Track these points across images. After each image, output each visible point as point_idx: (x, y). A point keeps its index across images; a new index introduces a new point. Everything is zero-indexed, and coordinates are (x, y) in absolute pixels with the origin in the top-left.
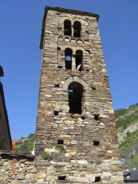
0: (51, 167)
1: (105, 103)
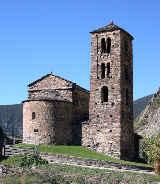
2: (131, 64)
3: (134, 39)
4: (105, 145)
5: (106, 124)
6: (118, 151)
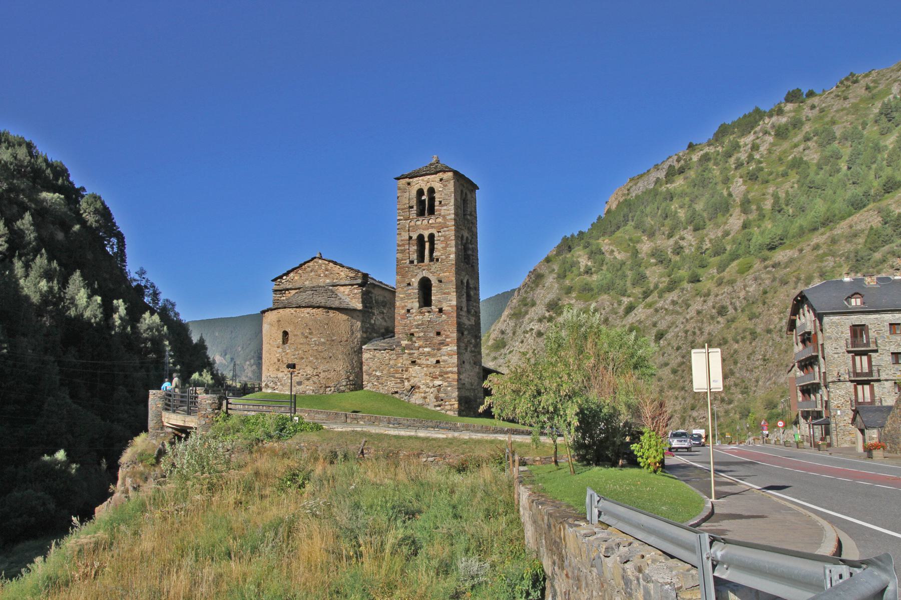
0: (406, 355)
2: (474, 235)
3: (478, 189)
4: (428, 390)
5: (427, 350)
6: (454, 400)
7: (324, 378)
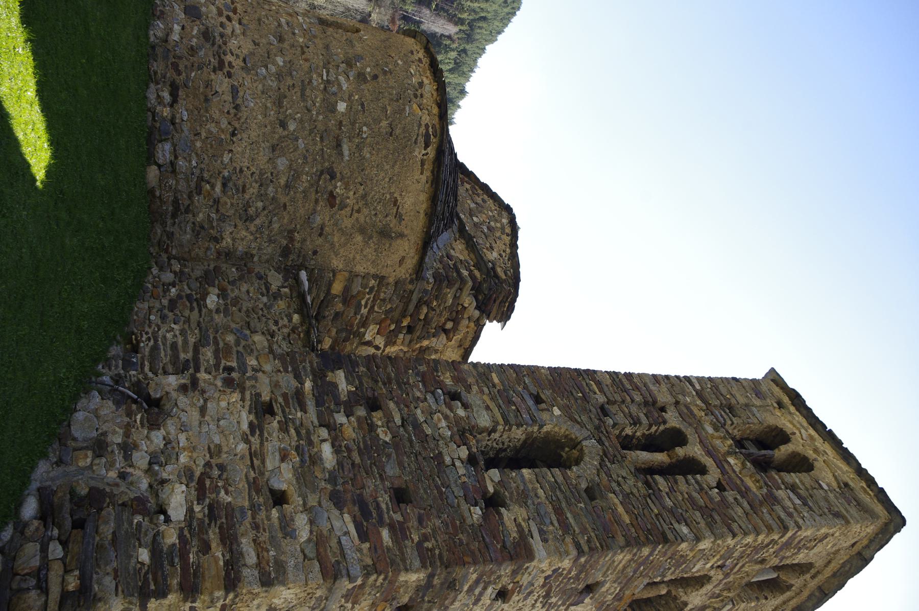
0: (294, 383)
1: (556, 524)
4: (141, 459)
7: (208, 84)
